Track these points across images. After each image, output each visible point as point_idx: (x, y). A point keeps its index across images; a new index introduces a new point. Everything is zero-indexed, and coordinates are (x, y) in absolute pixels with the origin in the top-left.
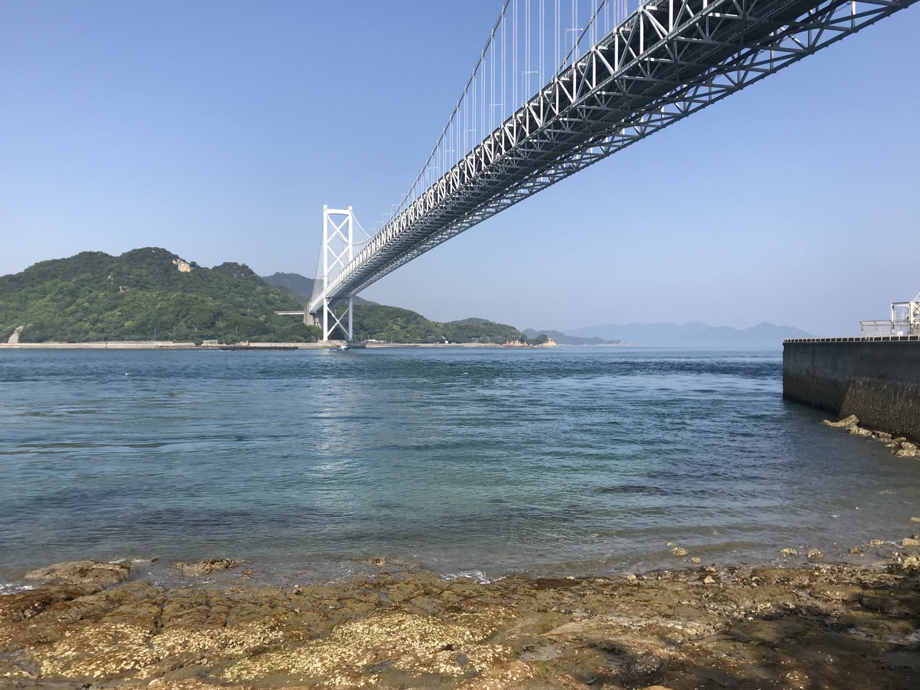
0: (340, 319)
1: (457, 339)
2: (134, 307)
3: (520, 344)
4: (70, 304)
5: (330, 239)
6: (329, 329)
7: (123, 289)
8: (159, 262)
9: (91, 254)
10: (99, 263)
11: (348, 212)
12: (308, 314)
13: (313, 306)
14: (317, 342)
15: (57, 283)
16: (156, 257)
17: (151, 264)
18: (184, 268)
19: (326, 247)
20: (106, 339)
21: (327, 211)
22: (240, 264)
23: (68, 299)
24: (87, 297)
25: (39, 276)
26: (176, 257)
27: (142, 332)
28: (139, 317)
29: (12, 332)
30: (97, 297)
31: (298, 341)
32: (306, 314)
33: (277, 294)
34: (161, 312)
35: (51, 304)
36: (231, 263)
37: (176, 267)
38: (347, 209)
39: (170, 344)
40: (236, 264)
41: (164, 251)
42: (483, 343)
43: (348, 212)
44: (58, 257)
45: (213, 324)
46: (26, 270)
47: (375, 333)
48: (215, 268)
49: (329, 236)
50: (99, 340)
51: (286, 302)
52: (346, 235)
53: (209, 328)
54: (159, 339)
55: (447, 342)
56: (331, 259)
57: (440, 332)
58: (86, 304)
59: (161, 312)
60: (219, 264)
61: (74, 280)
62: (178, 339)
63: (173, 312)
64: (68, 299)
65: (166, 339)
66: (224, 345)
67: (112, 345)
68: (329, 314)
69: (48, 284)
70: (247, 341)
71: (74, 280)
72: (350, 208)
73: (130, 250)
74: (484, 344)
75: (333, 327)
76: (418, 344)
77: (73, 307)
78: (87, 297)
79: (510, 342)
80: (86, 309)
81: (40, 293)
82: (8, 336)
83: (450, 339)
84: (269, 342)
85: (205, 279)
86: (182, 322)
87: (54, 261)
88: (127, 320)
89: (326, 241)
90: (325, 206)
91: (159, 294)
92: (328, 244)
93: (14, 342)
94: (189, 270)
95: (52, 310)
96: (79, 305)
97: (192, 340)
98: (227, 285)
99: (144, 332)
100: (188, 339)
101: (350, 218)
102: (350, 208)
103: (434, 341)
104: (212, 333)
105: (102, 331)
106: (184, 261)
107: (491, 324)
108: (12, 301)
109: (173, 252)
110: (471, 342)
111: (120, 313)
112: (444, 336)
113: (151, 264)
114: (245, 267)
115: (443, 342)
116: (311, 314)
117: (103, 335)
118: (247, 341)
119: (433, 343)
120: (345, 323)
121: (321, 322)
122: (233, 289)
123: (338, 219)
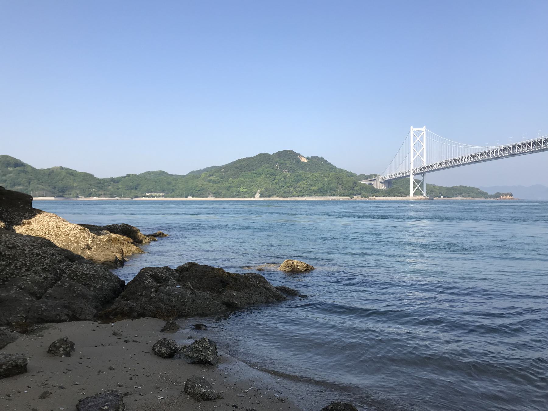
0: (419, 184)
1: (448, 196)
2: (311, 180)
3: (510, 198)
4: (275, 179)
7: (285, 171)
8: (293, 157)
9: (264, 154)
12: (378, 182)
16: (291, 155)
18: (303, 160)
19: (412, 148)
20: (302, 196)
21: (413, 130)
22: (320, 157)
23: (272, 177)
24: (281, 176)
25: (247, 166)
26: (299, 155)
27: (321, 192)
28: (320, 185)
29: (256, 193)
30: (286, 176)
32: (377, 182)
34: (329, 182)
35: (266, 179)
36: (315, 157)
38: (422, 127)
39: (338, 198)
40: (318, 157)
42: (465, 197)
43: (423, 129)
44: (249, 156)
46: (235, 161)
49: (414, 141)
50: (298, 196)
52: (422, 141)
53: (352, 190)
54: (330, 196)
55: (442, 197)
56: (415, 153)
57: (437, 191)
58: (283, 179)
59: (329, 182)
62: (340, 196)
63: (335, 182)
64: (272, 177)
65: (334, 195)
66: (364, 198)
67: (307, 198)
70: (374, 196)
72: (424, 127)
74: (466, 198)
77: (276, 181)
78: (281, 176)
80: (283, 182)
81: (258, 174)
82: (255, 195)
83: (444, 195)
84: (383, 196)
85: (317, 165)
86: (340, 187)
88: (311, 186)
89: (412, 145)
90: (412, 127)
91: (320, 174)
93: (257, 197)
94: (306, 161)
95: (268, 182)
96: (279, 180)
97: (347, 196)
98: (328, 168)
99: (322, 193)
100: (343, 195)
101: (424, 132)
102: (424, 127)
104: (354, 192)
105: (300, 192)
106: (303, 157)
107: (466, 187)
108: (247, 178)
109: (298, 152)
110: (457, 197)
111: (306, 183)
114: (322, 159)
115: (440, 197)
116: (380, 182)
117: (301, 194)
118: (374, 196)
122: (333, 170)
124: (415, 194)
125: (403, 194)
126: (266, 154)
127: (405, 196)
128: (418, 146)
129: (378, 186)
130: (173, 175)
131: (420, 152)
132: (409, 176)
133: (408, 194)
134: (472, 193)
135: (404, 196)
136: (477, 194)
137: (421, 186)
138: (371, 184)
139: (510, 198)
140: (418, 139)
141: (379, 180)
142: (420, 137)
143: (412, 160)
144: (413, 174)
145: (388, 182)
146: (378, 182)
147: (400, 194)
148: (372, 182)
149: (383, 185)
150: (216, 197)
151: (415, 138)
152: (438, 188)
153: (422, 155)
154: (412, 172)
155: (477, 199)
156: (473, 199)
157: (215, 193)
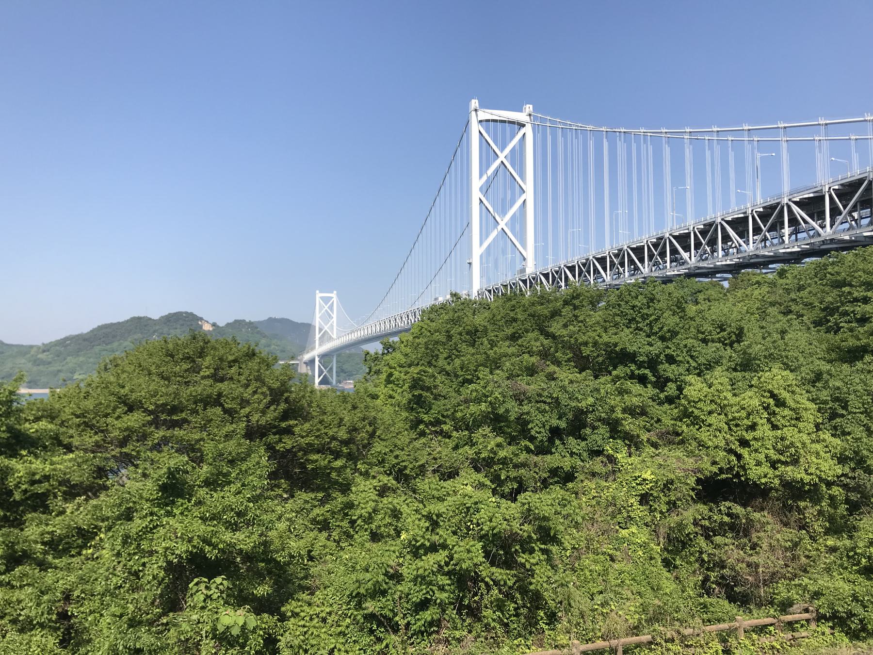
8: (189, 323)
9: (139, 318)
10: (145, 326)
11: (334, 295)
13: (307, 357)
15: (120, 345)
17: (183, 325)
18: (207, 327)
21: (319, 295)
22: (247, 321)
26: (201, 319)
37: (201, 327)
41: (192, 314)
43: (334, 295)
44: (115, 321)
47: (352, 375)
48: (228, 325)
49: (320, 312)
51: (284, 351)
52: (332, 310)
60: (231, 321)
61: (130, 340)
68: (319, 367)
69: (115, 344)
71: (130, 340)
72: (335, 292)
73: (167, 314)
87: (112, 325)
90: (317, 292)
92: (320, 317)
94: (211, 329)
101: (335, 299)
102: (335, 292)
106: (207, 322)
108: (90, 358)
109: (199, 315)
113: (183, 325)
116: (305, 363)
121: (313, 370)
123: (326, 300)
124: (321, 383)
126: (144, 317)
130: (12, 345)
140: (326, 307)
144: (319, 356)
150: (30, 388)
157: (29, 382)
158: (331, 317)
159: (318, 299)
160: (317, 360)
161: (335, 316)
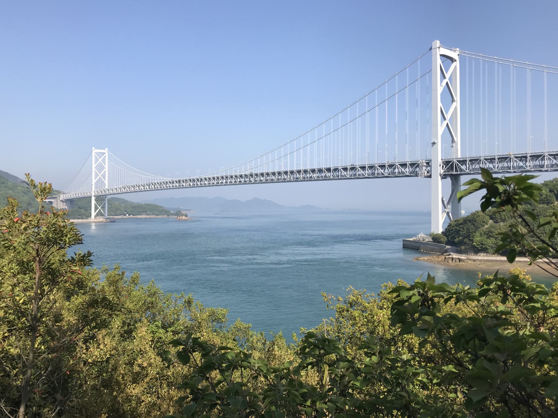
3: (186, 218)
5: (96, 164)
6: (95, 212)
11: (106, 151)
12: (59, 201)
14: (86, 218)
19: (94, 169)
21: (95, 151)
31: (78, 219)
32: (57, 201)
33: (22, 187)
38: (105, 150)
43: (106, 151)
45: (27, 209)
49: (96, 162)
52: (104, 162)
55: (127, 215)
56: (97, 175)
72: (107, 149)
75: (98, 210)
76: (113, 217)
79: (180, 217)
83: (129, 213)
90: (94, 148)
101: (107, 154)
102: (107, 149)
103: (120, 215)
107: (150, 205)
112: (126, 212)
115: (125, 215)
116: (61, 201)
119: (120, 215)
120: (103, 207)
122: (3, 185)
124: (97, 215)
125: (83, 216)
127: (86, 219)
128: (100, 168)
129: (59, 205)
131: (102, 174)
132: (91, 197)
133: (90, 216)
134: (156, 211)
135: (85, 218)
136: (160, 212)
137: (103, 207)
138: (51, 202)
139: (186, 218)
140: (100, 160)
141: (60, 198)
142: (102, 158)
143: (94, 181)
144: (95, 196)
145: (70, 202)
146: (59, 201)
147: (81, 216)
148: (52, 200)
149: (65, 204)
151: (97, 160)
152: (124, 206)
153: (104, 177)
154: (93, 194)
155: (160, 217)
156: (157, 217)
158: (104, 168)
159: (93, 153)
160: (93, 199)
161: (106, 167)
